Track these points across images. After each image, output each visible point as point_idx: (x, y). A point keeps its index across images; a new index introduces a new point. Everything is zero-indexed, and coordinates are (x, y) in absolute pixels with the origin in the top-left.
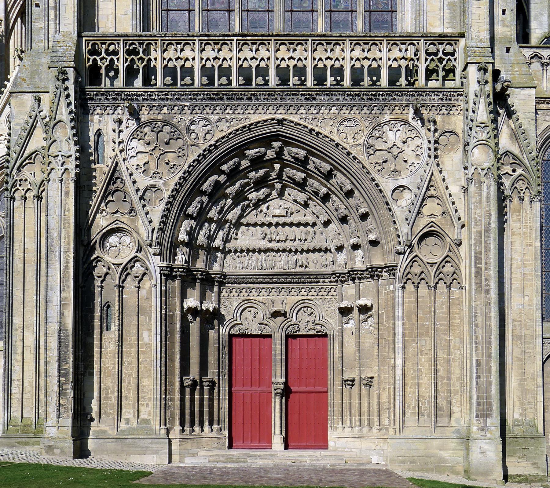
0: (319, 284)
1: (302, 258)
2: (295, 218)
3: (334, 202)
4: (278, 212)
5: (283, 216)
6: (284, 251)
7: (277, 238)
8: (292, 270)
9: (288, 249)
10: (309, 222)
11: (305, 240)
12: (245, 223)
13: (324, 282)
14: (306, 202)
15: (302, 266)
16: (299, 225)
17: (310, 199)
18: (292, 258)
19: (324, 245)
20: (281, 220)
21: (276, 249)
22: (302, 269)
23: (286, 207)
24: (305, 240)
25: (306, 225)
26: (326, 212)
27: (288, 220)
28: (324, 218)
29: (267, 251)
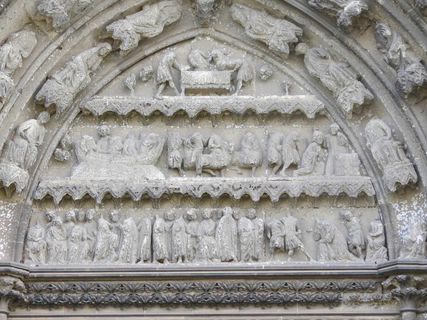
0: (342, 309)
1: (286, 223)
2: (262, 98)
3: (383, 43)
4: (203, 77)
5: (220, 92)
6: (225, 198)
7: (204, 160)
8: (251, 264)
9: (237, 195)
10: (304, 108)
11: (294, 166)
12: (100, 111)
13: (356, 302)
14: (293, 45)
15: (282, 250)
16: (274, 115)
17: (304, 37)
18: (251, 226)
19: (357, 180)
20: (214, 103)
21: (199, 194)
22: (280, 262)
23: (230, 63)
24: (294, 166)
25: (298, 115)
26: (360, 79)
27: (238, 100)
28: (353, 95)
29: (170, 196)
